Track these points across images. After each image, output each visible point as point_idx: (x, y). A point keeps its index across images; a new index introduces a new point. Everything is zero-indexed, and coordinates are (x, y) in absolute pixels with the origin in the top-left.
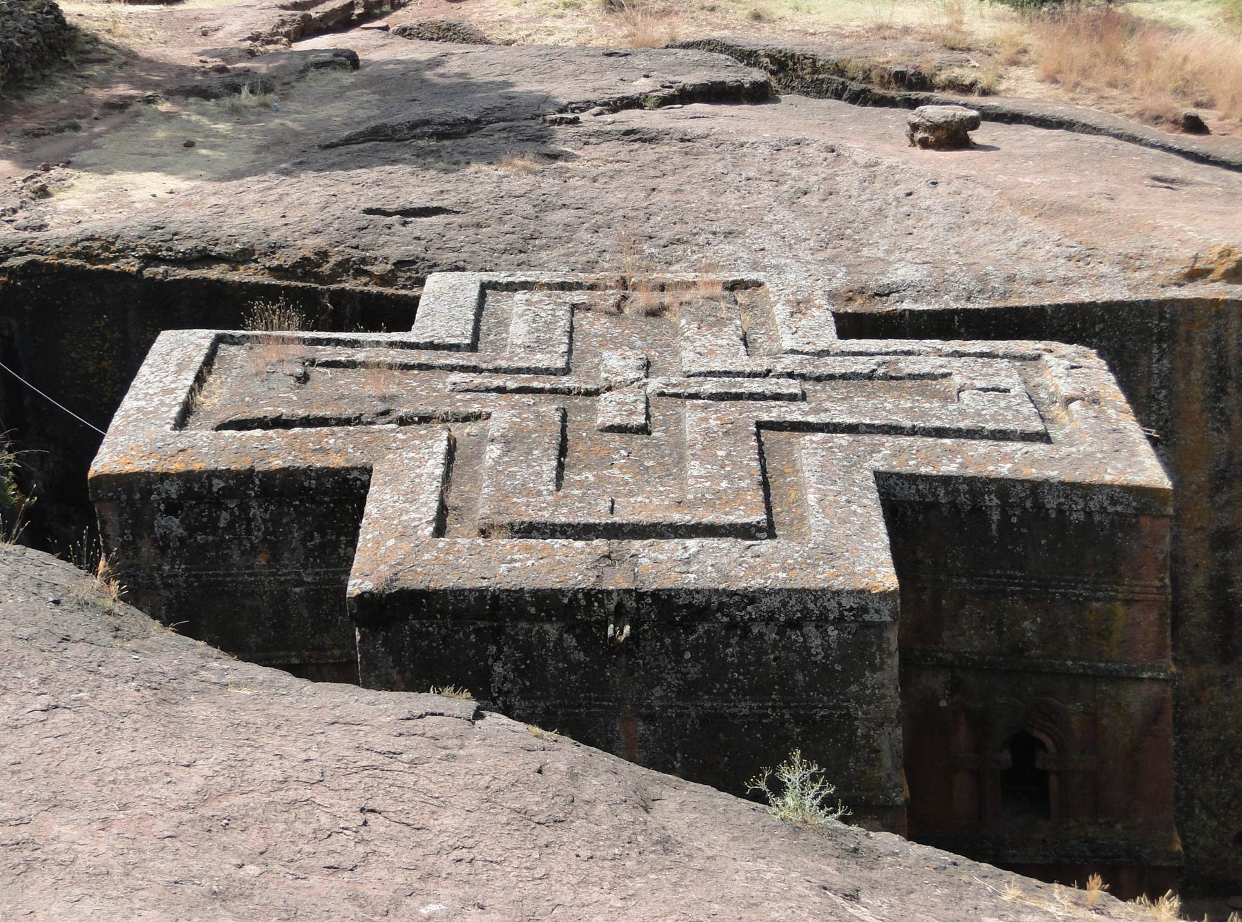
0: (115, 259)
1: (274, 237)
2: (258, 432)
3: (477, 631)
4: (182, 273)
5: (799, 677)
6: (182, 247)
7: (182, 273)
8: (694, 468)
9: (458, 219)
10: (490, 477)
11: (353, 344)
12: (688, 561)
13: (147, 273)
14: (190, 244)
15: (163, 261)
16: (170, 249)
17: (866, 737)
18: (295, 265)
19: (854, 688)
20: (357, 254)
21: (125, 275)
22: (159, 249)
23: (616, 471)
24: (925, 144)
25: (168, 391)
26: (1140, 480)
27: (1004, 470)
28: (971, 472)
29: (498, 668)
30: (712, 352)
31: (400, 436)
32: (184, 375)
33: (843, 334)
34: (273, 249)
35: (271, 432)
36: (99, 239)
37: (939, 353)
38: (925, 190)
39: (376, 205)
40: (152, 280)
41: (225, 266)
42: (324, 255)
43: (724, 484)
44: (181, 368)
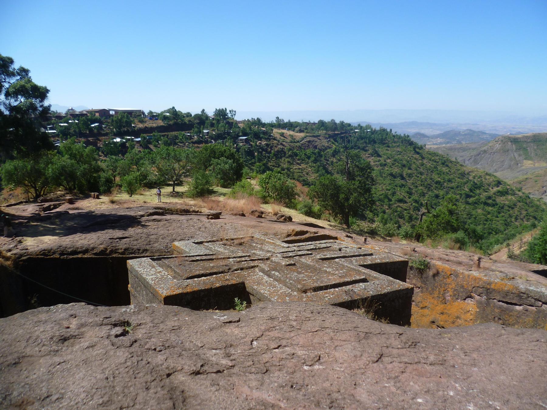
0: (52, 255)
1: (92, 246)
4: (71, 257)
6: (70, 250)
7: (71, 257)
9: (132, 239)
13: (62, 257)
14: (72, 249)
15: (65, 254)
16: (66, 251)
18: (100, 252)
20: (114, 248)
21: (57, 258)
22: (63, 251)
24: (212, 219)
34: (93, 249)
36: (47, 250)
38: (225, 225)
39: (111, 237)
40: (63, 259)
41: (82, 254)
42: (106, 249)
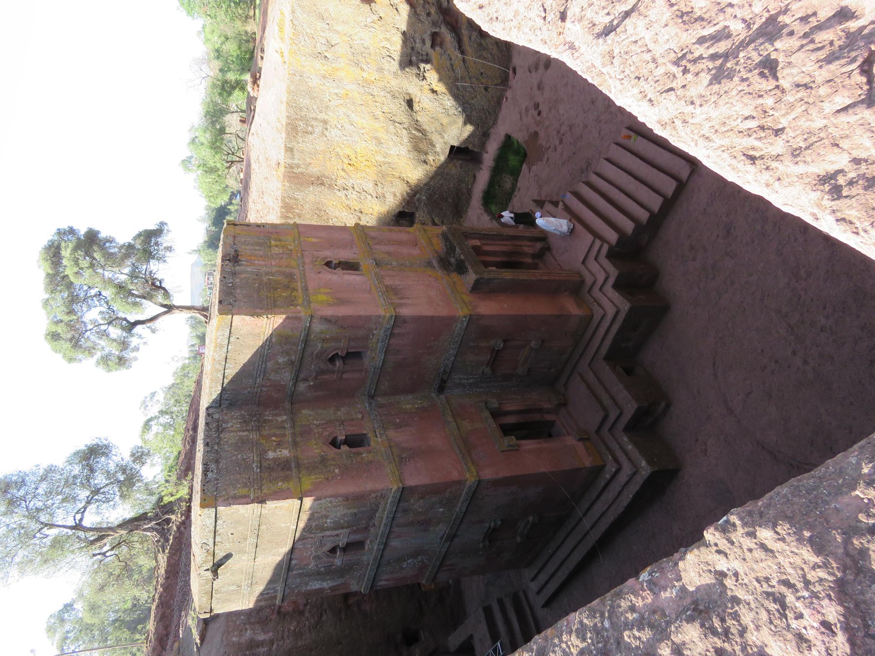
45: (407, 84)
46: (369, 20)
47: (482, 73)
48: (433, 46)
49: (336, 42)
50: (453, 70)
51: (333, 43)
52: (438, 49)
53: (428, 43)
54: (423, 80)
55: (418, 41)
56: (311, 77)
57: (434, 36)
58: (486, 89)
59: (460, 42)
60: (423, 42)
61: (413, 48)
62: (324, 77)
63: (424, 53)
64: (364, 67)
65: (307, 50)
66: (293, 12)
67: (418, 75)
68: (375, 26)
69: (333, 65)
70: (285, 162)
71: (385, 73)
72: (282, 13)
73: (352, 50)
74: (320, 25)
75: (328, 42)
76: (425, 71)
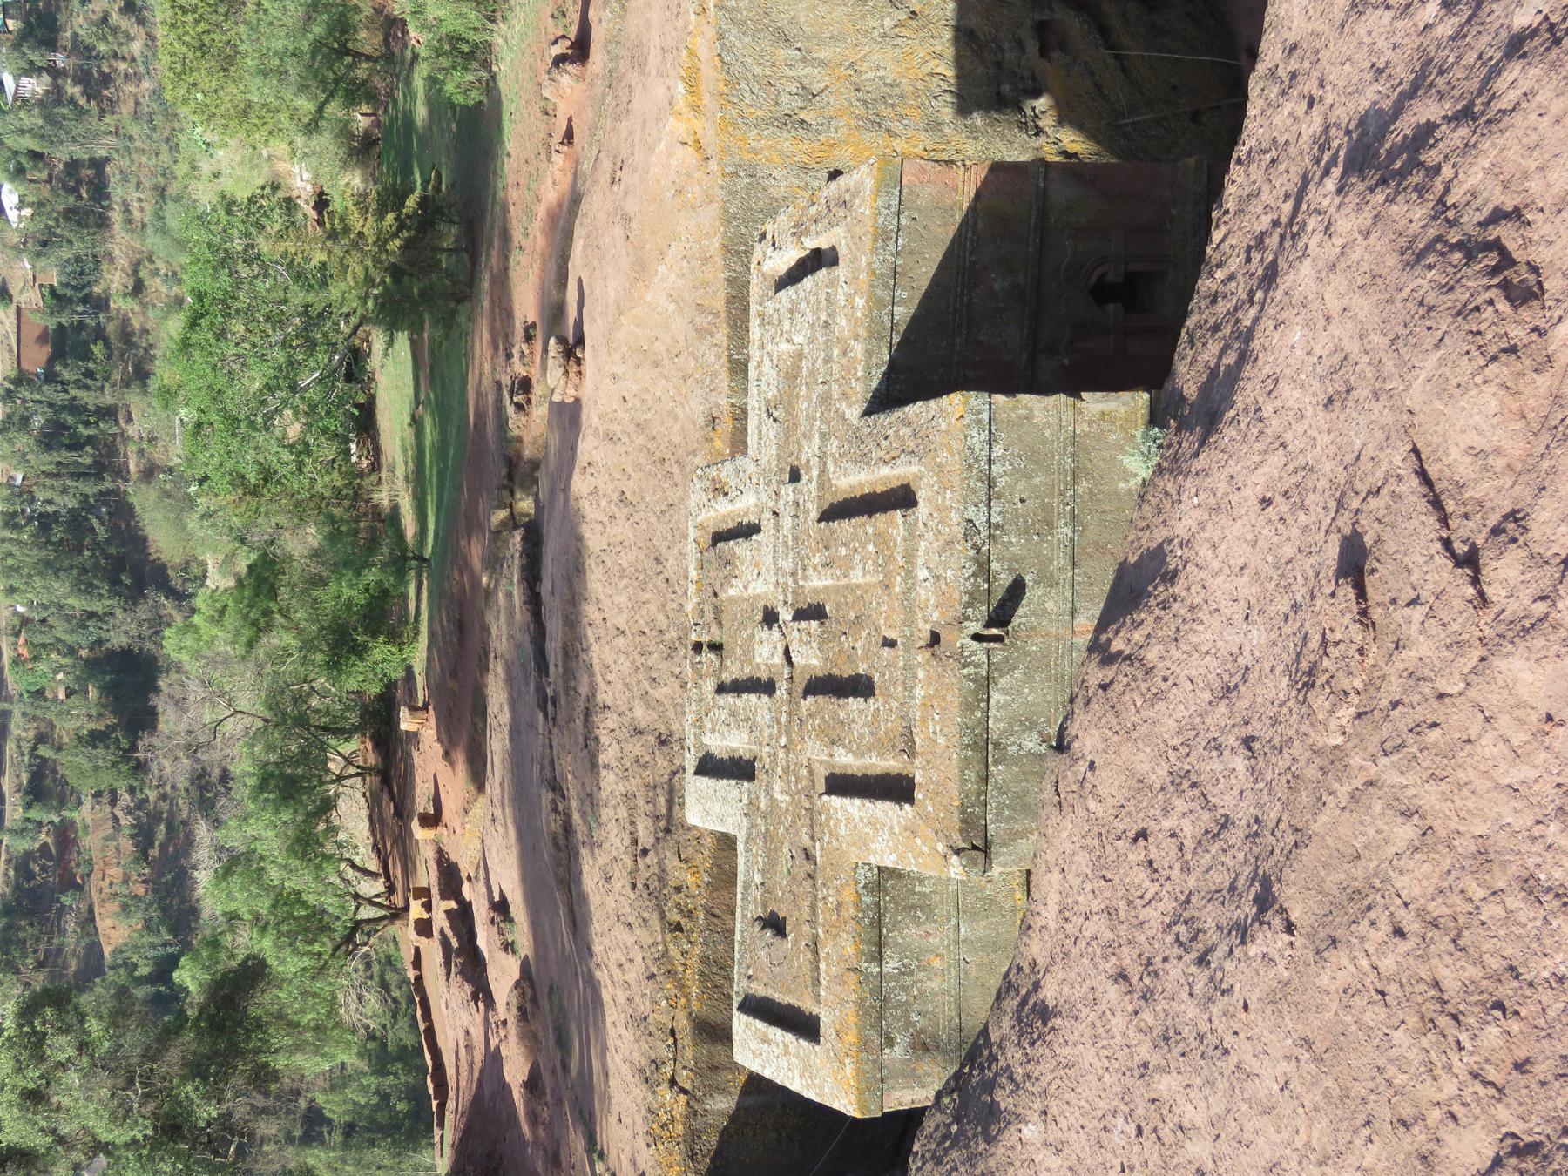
2: (823, 967)
3: (996, 763)
5: (1037, 481)
8: (857, 577)
10: (862, 756)
11: (746, 888)
12: (937, 577)
17: (1090, 424)
19: (1047, 433)
23: (858, 645)
25: (786, 1052)
26: (869, 184)
27: (860, 302)
28: (862, 332)
29: (1028, 745)
30: (756, 565)
31: (827, 838)
32: (771, 1036)
33: (744, 452)
35: (822, 955)
37: (759, 365)
43: (871, 547)
44: (766, 1040)
45: (1002, 148)
46: (888, 22)
47: (1175, 87)
48: (1044, 52)
49: (822, 85)
50: (1105, 97)
51: (815, 88)
52: (1056, 55)
53: (1032, 47)
54: (1037, 135)
55: (1006, 46)
56: (776, 174)
57: (1041, 28)
58: (1195, 116)
59: (1103, 30)
60: (1020, 46)
61: (998, 65)
62: (805, 168)
63: (1026, 74)
64: (897, 127)
65: (759, 113)
66: (721, 37)
67: (1023, 126)
68: (904, 32)
69: (823, 138)
70: (733, 405)
71: (947, 130)
72: (692, 54)
73: (860, 95)
74: (783, 53)
75: (803, 88)
76: (1036, 116)
